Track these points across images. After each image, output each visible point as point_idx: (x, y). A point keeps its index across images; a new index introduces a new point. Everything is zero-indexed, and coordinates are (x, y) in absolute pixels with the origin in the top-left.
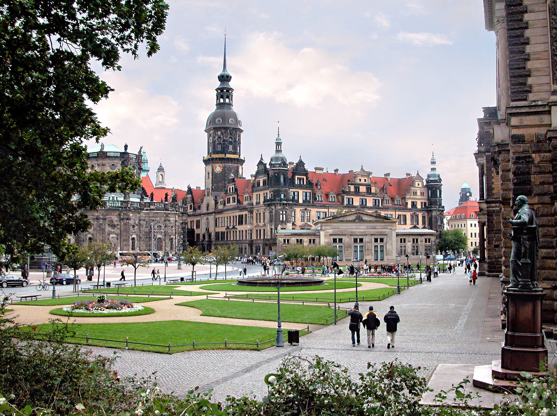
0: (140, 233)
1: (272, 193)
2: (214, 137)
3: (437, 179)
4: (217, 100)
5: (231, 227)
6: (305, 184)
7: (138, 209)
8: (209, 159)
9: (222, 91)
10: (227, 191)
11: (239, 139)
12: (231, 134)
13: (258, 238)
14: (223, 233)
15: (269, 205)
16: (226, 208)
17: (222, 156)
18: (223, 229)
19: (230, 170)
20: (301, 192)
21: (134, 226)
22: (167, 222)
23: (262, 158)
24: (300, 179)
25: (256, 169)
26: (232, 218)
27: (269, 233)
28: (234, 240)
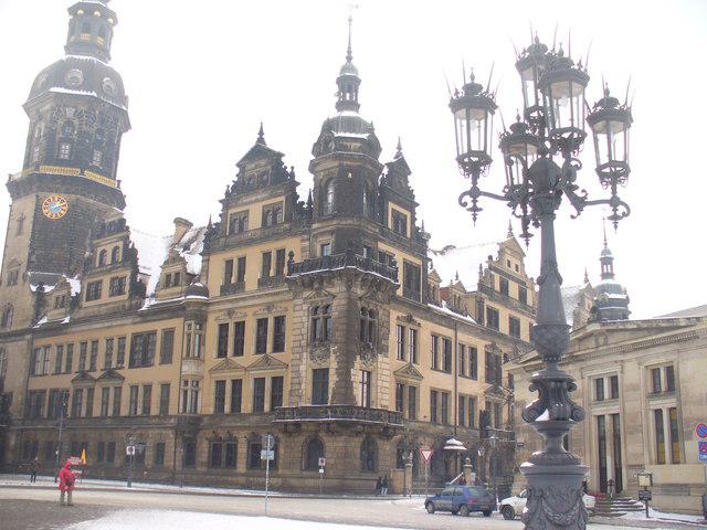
1: (331, 239)
3: (623, 297)
4: (72, 31)
5: (96, 375)
10: (91, 260)
11: (119, 141)
12: (102, 122)
13: (227, 409)
14: (59, 396)
15: (308, 283)
16: (81, 314)
17: (75, 172)
18: (65, 382)
20: (400, 257)
23: (261, 140)
24: (397, 216)
25: (230, 175)
26: (102, 347)
27: (307, 388)
28: (104, 417)
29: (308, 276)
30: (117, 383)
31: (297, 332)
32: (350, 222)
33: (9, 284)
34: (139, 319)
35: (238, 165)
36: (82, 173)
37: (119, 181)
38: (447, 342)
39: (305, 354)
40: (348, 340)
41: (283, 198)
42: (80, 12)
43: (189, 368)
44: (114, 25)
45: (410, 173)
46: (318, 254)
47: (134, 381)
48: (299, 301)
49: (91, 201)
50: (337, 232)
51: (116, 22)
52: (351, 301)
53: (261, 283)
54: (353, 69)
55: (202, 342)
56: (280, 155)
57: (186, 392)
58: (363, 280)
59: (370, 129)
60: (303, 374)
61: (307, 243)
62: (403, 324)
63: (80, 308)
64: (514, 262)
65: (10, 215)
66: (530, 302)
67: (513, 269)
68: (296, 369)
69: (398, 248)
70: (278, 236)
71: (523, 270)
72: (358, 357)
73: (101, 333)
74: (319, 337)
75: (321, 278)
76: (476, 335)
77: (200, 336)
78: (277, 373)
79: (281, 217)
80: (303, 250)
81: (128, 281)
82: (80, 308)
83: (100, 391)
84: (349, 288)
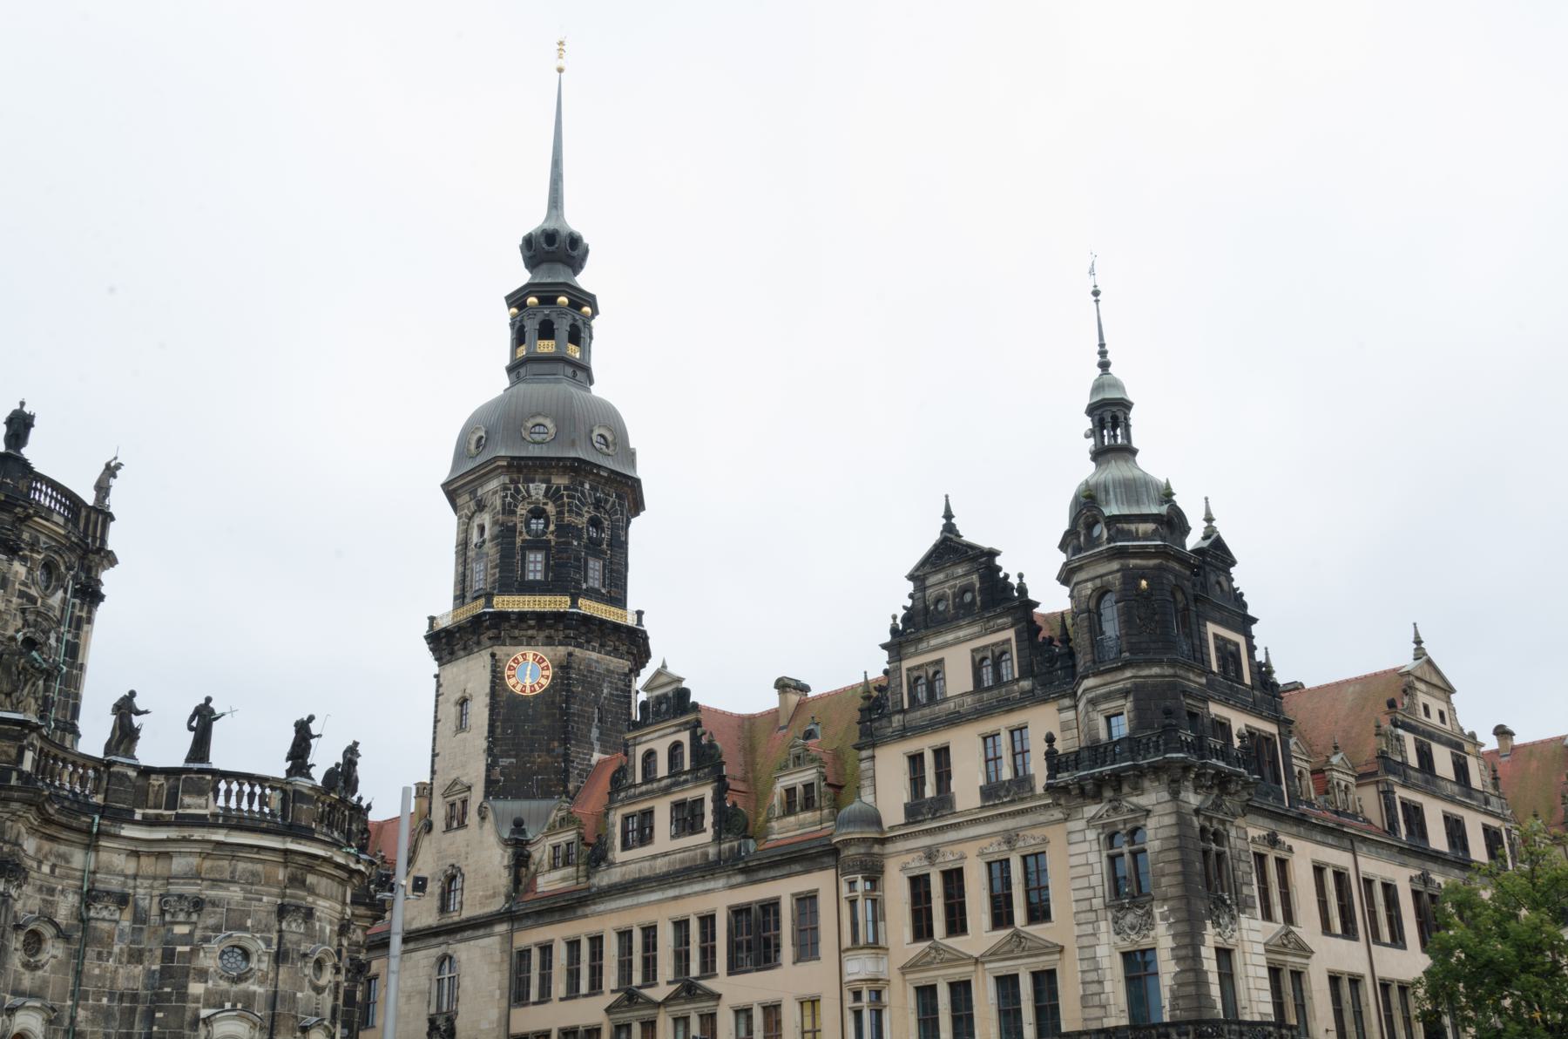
0: (79, 995)
1: (1128, 705)
2: (509, 510)
4: (519, 338)
5: (659, 993)
6: (1247, 680)
7: (82, 806)
8: (476, 622)
9: (547, 300)
12: (598, 505)
15: (1092, 791)
16: (604, 878)
17: (561, 603)
19: (591, 680)
20: (1239, 721)
21: (34, 942)
22: (294, 927)
23: (949, 528)
25: (899, 597)
29: (1086, 777)
30: (706, 1006)
31: (1084, 883)
32: (1155, 670)
33: (449, 828)
34: (740, 879)
35: (911, 577)
36: (574, 604)
37: (640, 614)
38: (1340, 876)
39: (1103, 925)
40: (1187, 896)
41: (1010, 634)
42: (532, 300)
43: (860, 967)
44: (593, 317)
45: (1233, 563)
46: (1103, 736)
47: (742, 1000)
48: (1081, 824)
49: (594, 655)
50: (1136, 692)
51: (595, 312)
52: (1182, 821)
53: (991, 792)
54: (1117, 385)
55: (878, 915)
56: (993, 554)
57: (858, 1014)
58: (1198, 776)
59: (1167, 496)
60: (1105, 963)
61: (1071, 715)
62: (1262, 850)
63: (611, 864)
64: (1436, 705)
65: (438, 696)
66: (1476, 781)
67: (1435, 720)
68: (1088, 953)
69: (1233, 707)
70: (1009, 705)
71: (1454, 719)
72: (1209, 923)
73: (661, 910)
74: (1127, 892)
75: (1117, 781)
76: (1390, 859)
77: (874, 901)
78: (1042, 963)
79: (1011, 669)
80: (1065, 727)
81: (708, 807)
82: (611, 864)
83: (670, 1022)
84: (1175, 795)
